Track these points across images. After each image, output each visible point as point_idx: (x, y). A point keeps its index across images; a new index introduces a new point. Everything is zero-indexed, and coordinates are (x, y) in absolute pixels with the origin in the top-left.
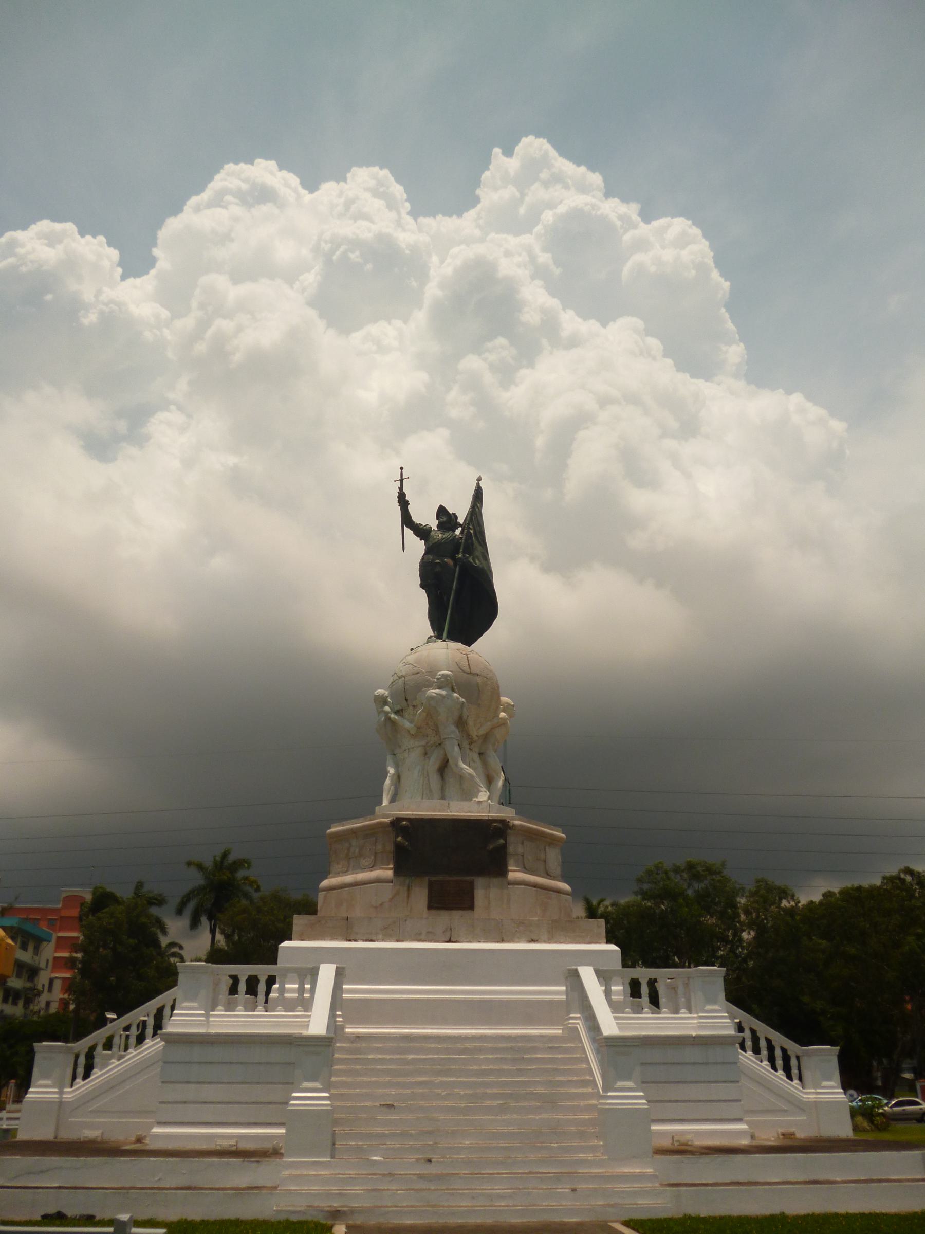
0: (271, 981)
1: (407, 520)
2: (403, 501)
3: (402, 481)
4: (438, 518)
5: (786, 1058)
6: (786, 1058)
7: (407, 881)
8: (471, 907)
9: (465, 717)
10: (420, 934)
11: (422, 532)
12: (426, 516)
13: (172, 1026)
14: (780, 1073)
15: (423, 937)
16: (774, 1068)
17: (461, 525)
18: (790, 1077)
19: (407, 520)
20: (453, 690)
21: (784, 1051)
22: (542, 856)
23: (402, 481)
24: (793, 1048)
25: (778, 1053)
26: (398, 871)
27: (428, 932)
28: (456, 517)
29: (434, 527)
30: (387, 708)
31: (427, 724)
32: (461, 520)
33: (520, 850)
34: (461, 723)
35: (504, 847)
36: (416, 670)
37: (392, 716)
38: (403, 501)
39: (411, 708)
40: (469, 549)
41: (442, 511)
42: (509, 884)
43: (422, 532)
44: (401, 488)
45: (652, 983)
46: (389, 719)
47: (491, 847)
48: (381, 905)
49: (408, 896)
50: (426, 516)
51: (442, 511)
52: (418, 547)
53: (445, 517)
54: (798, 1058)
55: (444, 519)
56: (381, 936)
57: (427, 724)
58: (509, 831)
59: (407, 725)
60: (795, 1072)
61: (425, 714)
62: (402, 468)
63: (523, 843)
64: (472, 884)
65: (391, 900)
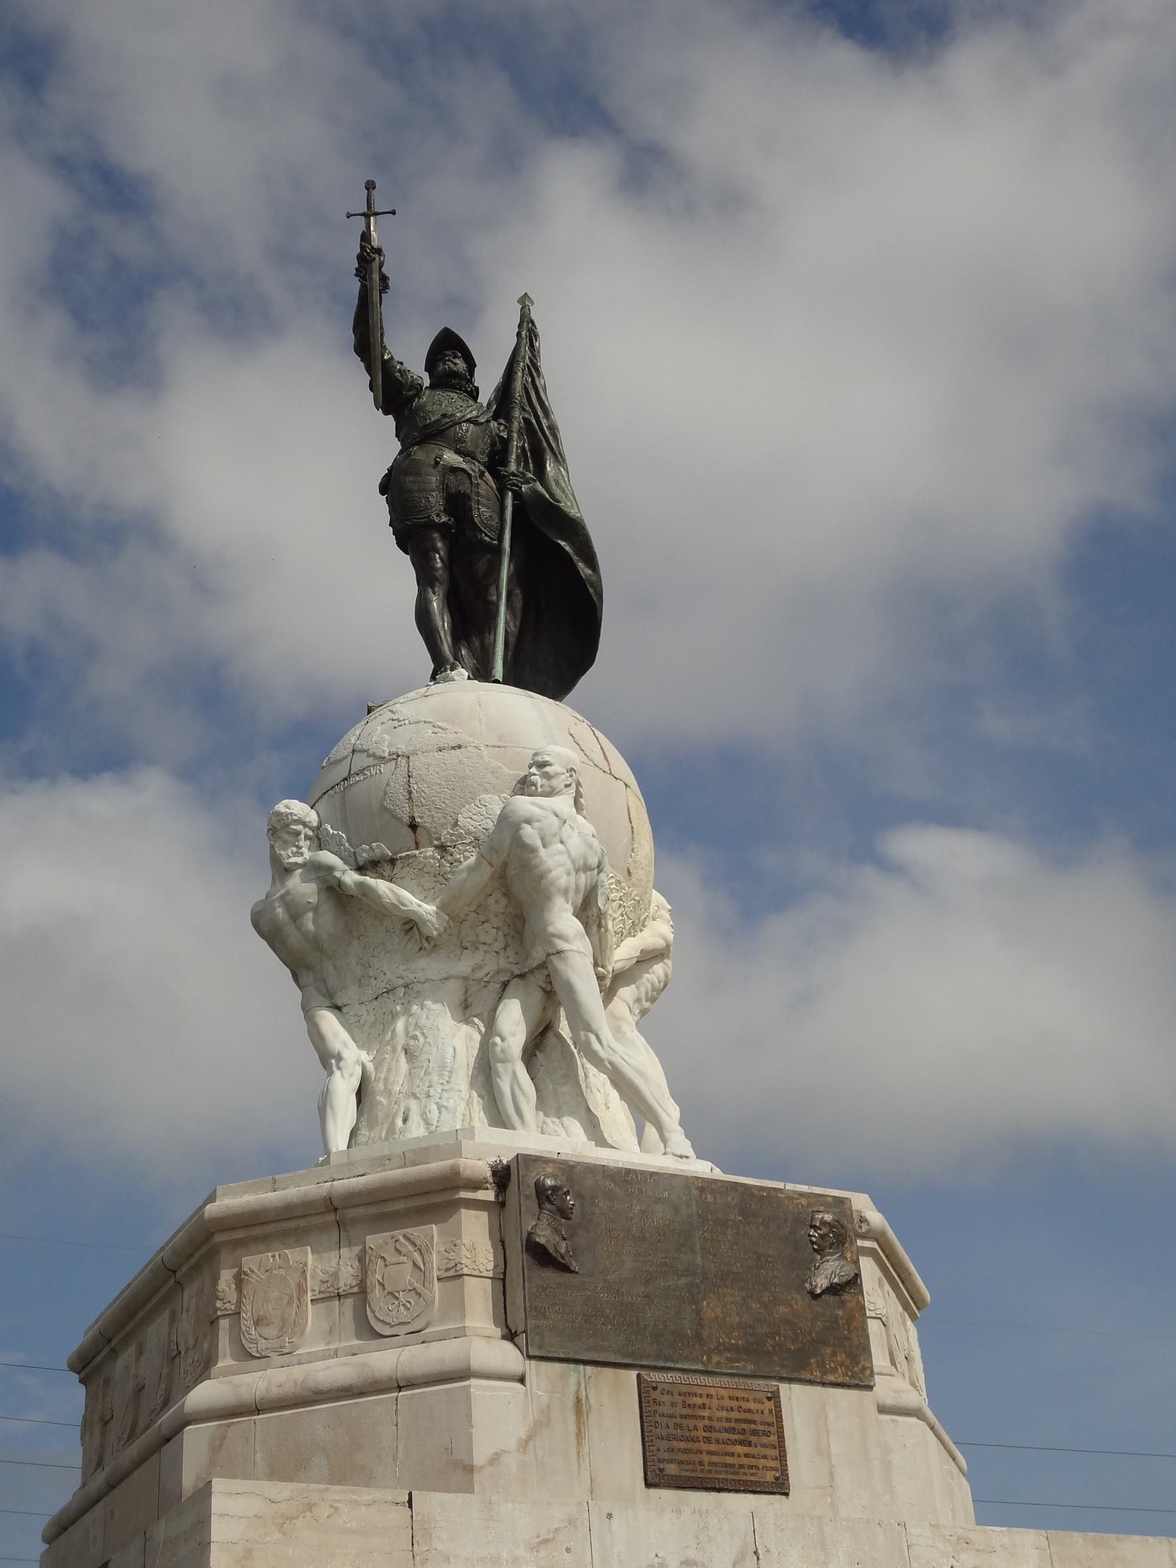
7: (573, 1380)
8: (780, 1487)
30: (328, 857)
36: (452, 739)
37: (351, 878)
39: (430, 851)
46: (334, 890)
47: (821, 1283)
48: (495, 1459)
49: (579, 1435)
61: (487, 871)
62: (370, 186)
64: (775, 1397)
65: (525, 1444)
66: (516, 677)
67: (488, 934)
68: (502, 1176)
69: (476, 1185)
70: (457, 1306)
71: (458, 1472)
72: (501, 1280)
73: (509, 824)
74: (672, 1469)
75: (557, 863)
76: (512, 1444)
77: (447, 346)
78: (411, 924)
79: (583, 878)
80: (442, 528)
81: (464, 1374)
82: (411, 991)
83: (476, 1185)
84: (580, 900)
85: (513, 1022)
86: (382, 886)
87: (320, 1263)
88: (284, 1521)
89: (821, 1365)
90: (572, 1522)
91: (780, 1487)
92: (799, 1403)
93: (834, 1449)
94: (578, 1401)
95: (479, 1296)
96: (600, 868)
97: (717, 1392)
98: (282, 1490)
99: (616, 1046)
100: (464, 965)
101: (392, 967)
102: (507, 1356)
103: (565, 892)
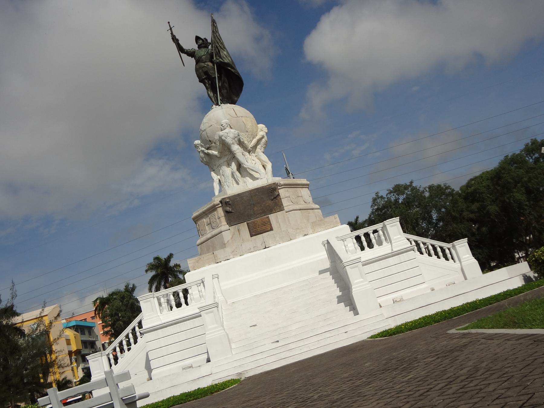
0: (186, 292)
1: (181, 49)
2: (175, 40)
3: (171, 29)
4: (197, 43)
5: (443, 251)
6: (443, 251)
8: (271, 229)
11: (191, 54)
12: (190, 44)
13: (145, 326)
14: (443, 259)
15: (252, 250)
16: (439, 257)
17: (210, 44)
18: (447, 259)
19: (181, 49)
20: (231, 128)
21: (441, 248)
22: (300, 195)
23: (171, 29)
24: (445, 245)
25: (439, 250)
28: (206, 40)
29: (197, 48)
31: (224, 150)
32: (209, 41)
34: (241, 143)
35: (279, 195)
36: (210, 125)
37: (206, 151)
38: (175, 40)
40: (218, 54)
41: (197, 38)
44: (172, 34)
45: (367, 235)
46: (205, 153)
50: (190, 44)
51: (197, 38)
52: (191, 62)
53: (201, 42)
54: (449, 249)
55: (201, 41)
57: (224, 150)
58: (279, 188)
59: (215, 153)
60: (449, 256)
62: (169, 23)
64: (268, 218)
65: (232, 238)
66: (223, 102)
67: (227, 153)
68: (221, 202)
69: (218, 205)
70: (221, 222)
71: (223, 245)
72: (225, 216)
73: (220, 137)
74: (254, 234)
75: (229, 140)
76: (230, 239)
78: (216, 156)
79: (236, 139)
80: (206, 78)
81: (221, 232)
82: (220, 166)
83: (218, 205)
84: (238, 142)
85: (234, 166)
86: (210, 151)
87: (205, 220)
88: (197, 262)
89: (275, 210)
91: (271, 229)
92: (272, 217)
95: (223, 220)
97: (258, 220)
98: (196, 258)
99: (248, 164)
100: (226, 159)
101: (218, 163)
102: (227, 227)
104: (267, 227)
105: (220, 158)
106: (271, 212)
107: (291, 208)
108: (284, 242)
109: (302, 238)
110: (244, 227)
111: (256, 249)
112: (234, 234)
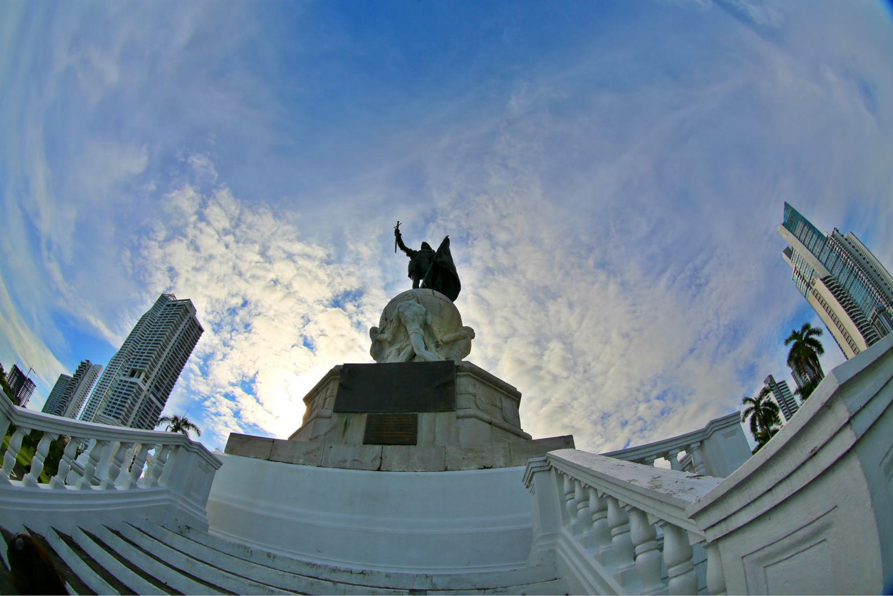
8: (413, 442)
9: (429, 323)
10: (345, 461)
15: (348, 464)
22: (499, 404)
26: (337, 410)
27: (355, 460)
33: (471, 389)
34: (426, 326)
42: (458, 418)
43: (409, 253)
48: (317, 437)
56: (301, 461)
63: (474, 385)
64: (415, 418)
65: (326, 434)
77: (425, 246)
79: (421, 318)
90: (318, 449)
91: (413, 442)
93: (437, 429)
94: (346, 423)
96: (426, 314)
103: (413, 321)
104: (406, 435)
105: (392, 343)
106: (425, 409)
107: (472, 411)
108: (426, 470)
109: (473, 472)
110: (359, 425)
111: (357, 464)
112: (334, 428)
